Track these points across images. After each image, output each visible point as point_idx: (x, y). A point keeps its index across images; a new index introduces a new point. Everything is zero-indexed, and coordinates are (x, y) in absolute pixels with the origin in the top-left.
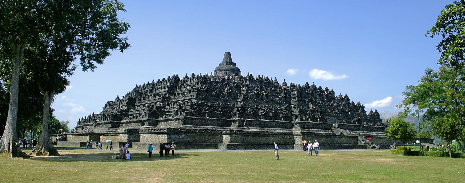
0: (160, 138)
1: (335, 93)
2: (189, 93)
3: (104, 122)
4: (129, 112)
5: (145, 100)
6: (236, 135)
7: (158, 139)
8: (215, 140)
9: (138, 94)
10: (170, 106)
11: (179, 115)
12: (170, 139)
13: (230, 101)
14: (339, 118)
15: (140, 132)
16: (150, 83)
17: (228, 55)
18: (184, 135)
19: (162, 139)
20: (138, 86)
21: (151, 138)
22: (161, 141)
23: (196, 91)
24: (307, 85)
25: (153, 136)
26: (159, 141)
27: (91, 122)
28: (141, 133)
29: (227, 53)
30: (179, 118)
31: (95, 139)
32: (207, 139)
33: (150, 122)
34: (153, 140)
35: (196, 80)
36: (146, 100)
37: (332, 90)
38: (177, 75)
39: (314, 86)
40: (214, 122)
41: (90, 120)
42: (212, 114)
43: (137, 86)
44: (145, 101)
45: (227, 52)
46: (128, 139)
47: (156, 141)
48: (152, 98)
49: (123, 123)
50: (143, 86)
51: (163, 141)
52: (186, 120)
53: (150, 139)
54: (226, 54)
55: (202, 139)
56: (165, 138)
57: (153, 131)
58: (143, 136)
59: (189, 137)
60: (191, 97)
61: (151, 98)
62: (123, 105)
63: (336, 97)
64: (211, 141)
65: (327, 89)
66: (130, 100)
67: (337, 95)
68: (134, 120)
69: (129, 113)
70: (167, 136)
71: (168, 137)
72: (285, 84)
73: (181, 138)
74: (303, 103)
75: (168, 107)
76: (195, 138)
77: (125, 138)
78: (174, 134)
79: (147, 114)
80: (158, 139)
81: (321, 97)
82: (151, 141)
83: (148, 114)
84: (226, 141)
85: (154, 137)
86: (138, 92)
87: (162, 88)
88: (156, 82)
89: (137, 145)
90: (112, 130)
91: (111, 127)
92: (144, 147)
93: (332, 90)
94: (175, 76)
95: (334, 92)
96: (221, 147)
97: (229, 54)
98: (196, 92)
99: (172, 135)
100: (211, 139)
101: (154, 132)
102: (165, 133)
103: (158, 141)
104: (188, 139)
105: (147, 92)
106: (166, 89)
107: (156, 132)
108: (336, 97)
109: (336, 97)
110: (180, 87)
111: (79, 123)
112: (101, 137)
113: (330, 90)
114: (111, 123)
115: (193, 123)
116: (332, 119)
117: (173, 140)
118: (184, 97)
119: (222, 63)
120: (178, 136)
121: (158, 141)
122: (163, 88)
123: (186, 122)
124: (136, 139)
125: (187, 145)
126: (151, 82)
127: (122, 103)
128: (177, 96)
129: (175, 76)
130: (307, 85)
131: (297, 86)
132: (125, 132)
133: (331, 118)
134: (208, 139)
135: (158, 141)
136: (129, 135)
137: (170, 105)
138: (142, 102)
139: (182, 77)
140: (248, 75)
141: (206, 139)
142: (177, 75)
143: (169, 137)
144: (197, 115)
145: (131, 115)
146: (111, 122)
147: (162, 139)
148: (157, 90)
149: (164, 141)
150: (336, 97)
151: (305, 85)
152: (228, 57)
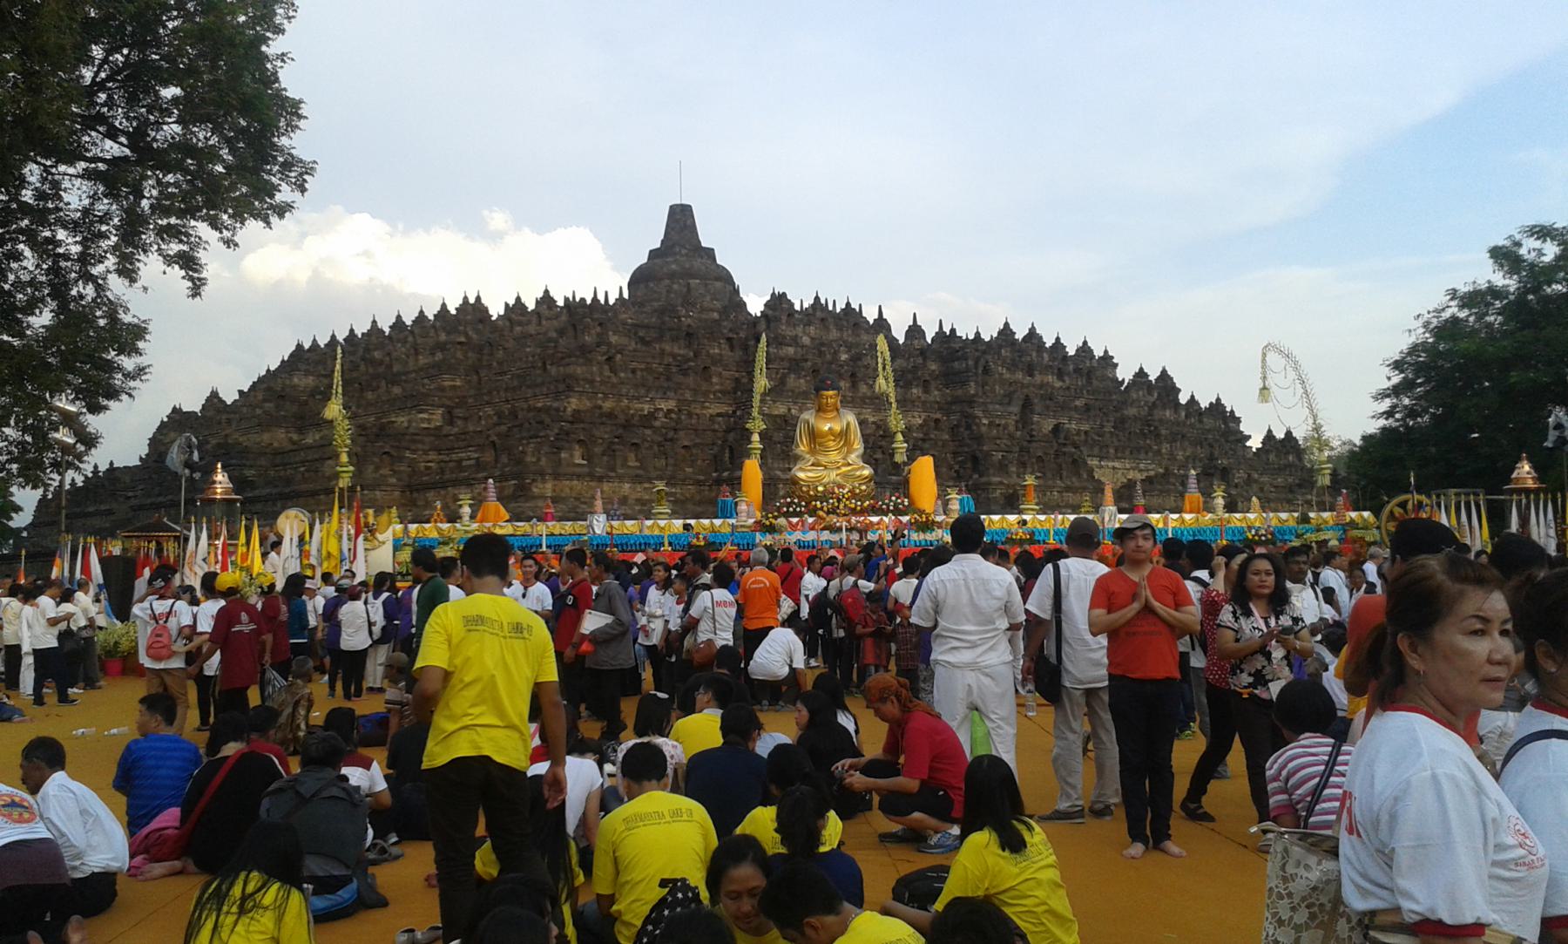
1: (1117, 365)
13: (707, 404)
14: (1142, 466)
16: (359, 333)
20: (307, 346)
24: (1006, 331)
33: (377, 493)
37: (1106, 352)
38: (478, 299)
39: (1032, 335)
40: (645, 488)
42: (636, 456)
43: (299, 347)
50: (326, 345)
52: (534, 480)
63: (1120, 379)
65: (1085, 349)
67: (1125, 373)
72: (915, 331)
74: (997, 406)
81: (1064, 381)
93: (1106, 352)
94: (472, 300)
95: (1115, 361)
108: (1123, 380)
109: (1123, 380)
113: (1098, 353)
115: (563, 495)
116: (1114, 468)
123: (535, 490)
126: (361, 329)
129: (472, 300)
130: (1006, 331)
131: (971, 337)
133: (1110, 464)
139: (496, 310)
140: (773, 294)
142: (478, 299)
144: (577, 462)
150: (1120, 379)
151: (1000, 333)
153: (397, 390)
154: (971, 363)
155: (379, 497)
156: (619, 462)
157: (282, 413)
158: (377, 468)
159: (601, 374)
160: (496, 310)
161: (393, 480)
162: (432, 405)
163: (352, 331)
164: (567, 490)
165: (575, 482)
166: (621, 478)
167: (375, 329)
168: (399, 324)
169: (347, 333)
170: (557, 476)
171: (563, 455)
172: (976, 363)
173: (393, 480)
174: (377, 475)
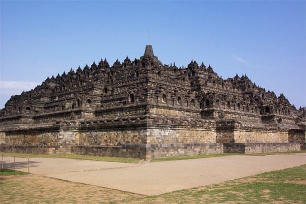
0: (128, 136)
6: (240, 129)
7: (124, 136)
8: (208, 137)
12: (152, 136)
17: (149, 49)
21: (106, 136)
22: (130, 141)
26: (126, 140)
32: (199, 137)
34: (110, 139)
38: (106, 60)
47: (118, 140)
51: (137, 141)
53: (102, 137)
55: (194, 136)
56: (140, 136)
59: (178, 133)
64: (204, 139)
73: (167, 134)
76: (185, 134)
78: (158, 127)
80: (124, 136)
84: (226, 139)
85: (113, 134)
92: (101, 153)
94: (104, 61)
96: (230, 149)
97: (150, 46)
100: (204, 137)
103: (124, 140)
104: (176, 136)
117: (157, 138)
120: (163, 132)
121: (122, 140)
124: (74, 139)
125: (186, 148)
134: (201, 136)
141: (198, 137)
142: (106, 60)
147: (134, 136)
149: (140, 141)
153: (85, 84)
154: (245, 83)
156: (175, 103)
158: (85, 105)
159: (157, 77)
160: (111, 65)
161: (91, 109)
163: (64, 73)
164: (160, 112)
165: (162, 109)
166: (176, 109)
169: (63, 73)
170: (158, 107)
171: (159, 99)
172: (247, 84)
173: (91, 109)
174: (86, 107)
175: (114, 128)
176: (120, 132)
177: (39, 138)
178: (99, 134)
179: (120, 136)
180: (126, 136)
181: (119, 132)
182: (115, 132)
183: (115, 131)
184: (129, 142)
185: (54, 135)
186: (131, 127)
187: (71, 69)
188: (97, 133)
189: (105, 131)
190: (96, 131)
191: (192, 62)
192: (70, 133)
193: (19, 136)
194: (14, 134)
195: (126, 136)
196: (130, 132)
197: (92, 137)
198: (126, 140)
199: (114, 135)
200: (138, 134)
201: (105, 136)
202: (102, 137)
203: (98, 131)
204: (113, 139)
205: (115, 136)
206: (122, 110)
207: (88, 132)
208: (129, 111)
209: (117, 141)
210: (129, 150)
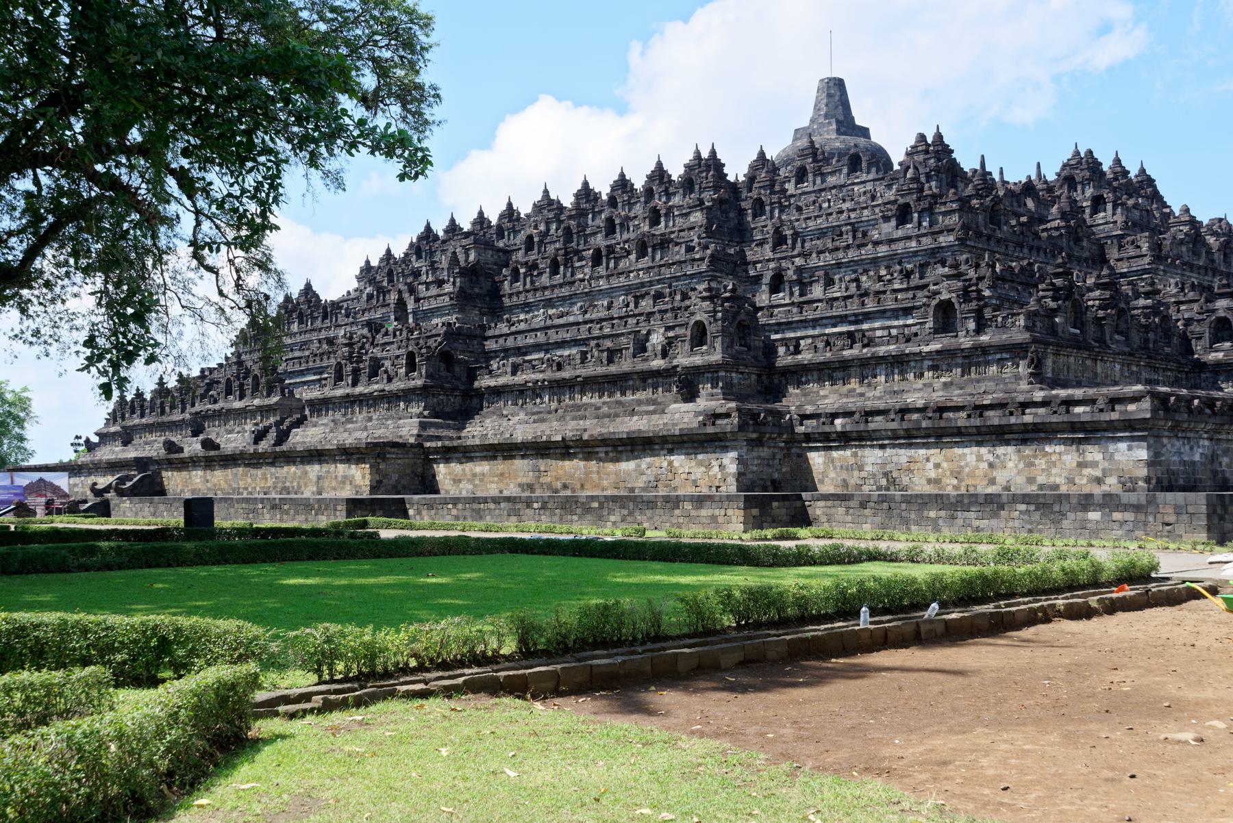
2: (893, 223)
3: (359, 389)
4: (487, 339)
5: (569, 274)
9: (490, 252)
10: (792, 294)
11: (972, 325)
15: (800, 429)
18: (1207, 443)
19: (1081, 465)
21: (937, 466)
23: (953, 211)
25: (958, 451)
27: (253, 397)
28: (808, 437)
29: (831, 84)
30: (975, 348)
31: (404, 482)
33: (734, 375)
35: (845, 170)
36: (573, 274)
38: (713, 153)
41: (242, 385)
44: (568, 278)
45: (830, 79)
46: (740, 476)
48: (621, 265)
49: (498, 392)
54: (829, 88)
57: (963, 414)
58: (835, 454)
60: (914, 244)
61: (612, 265)
62: (425, 306)
66: (471, 281)
68: (591, 370)
69: (491, 345)
70: (1148, 448)
71: (1152, 454)
75: (782, 297)
77: (709, 466)
79: (712, 329)
80: (1032, 464)
82: (937, 481)
83: (723, 331)
86: (489, 245)
87: (660, 216)
88: (494, 221)
89: (867, 512)
90: (432, 432)
91: (426, 413)
97: (839, 84)
98: (945, 214)
99: (1165, 441)
101: (977, 422)
102: (1130, 425)
103: (1031, 480)
105: (541, 242)
106: (692, 219)
107: (1013, 420)
110: (768, 208)
111: (142, 406)
112: (442, 471)
114: (422, 392)
118: (848, 247)
119: (808, 128)
121: (1020, 480)
122: (666, 215)
124: (776, 476)
127: (422, 295)
128: (793, 248)
132: (710, 430)
135: (1031, 480)
136: (745, 449)
137: (796, 290)
138: (545, 288)
142: (713, 153)
143: (1157, 454)
145: (507, 352)
146: (425, 388)
147: (1081, 465)
148: (622, 225)
152: (837, 98)
155: (735, 381)
157: (477, 290)
162: (721, 272)
167: (510, 213)
168: (548, 204)
175: (979, 434)
176: (1010, 449)
177: (617, 473)
178: (902, 456)
179: (1010, 464)
180: (1041, 463)
181: (1001, 450)
182: (984, 450)
183: (980, 444)
184: (1057, 487)
185: (700, 464)
186: (1063, 431)
187: (546, 192)
188: (889, 451)
189: (926, 446)
190: (882, 447)
191: (1077, 153)
192: (765, 452)
193: (500, 466)
194: (470, 459)
195: (1041, 463)
196: (1060, 448)
197: (861, 468)
198: (1041, 479)
199: (980, 458)
200: (1098, 457)
201: (930, 465)
202: (912, 466)
203: (894, 446)
204: (971, 475)
205: (985, 465)
206: (902, 363)
207: (837, 448)
208: (934, 368)
209: (992, 482)
210: (1117, 516)
